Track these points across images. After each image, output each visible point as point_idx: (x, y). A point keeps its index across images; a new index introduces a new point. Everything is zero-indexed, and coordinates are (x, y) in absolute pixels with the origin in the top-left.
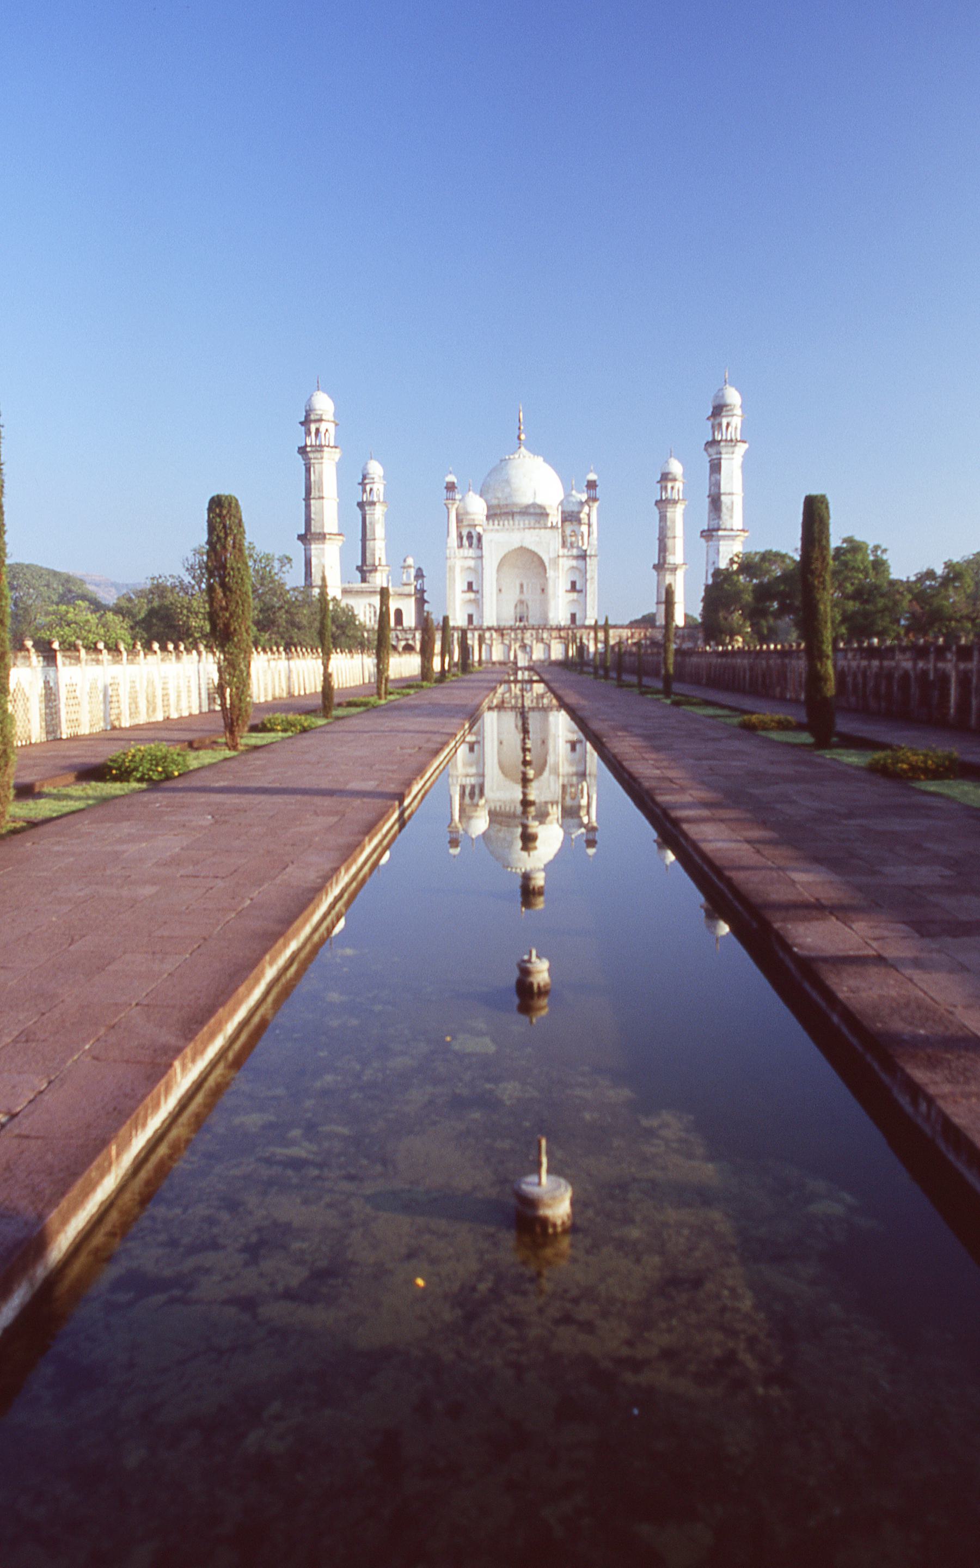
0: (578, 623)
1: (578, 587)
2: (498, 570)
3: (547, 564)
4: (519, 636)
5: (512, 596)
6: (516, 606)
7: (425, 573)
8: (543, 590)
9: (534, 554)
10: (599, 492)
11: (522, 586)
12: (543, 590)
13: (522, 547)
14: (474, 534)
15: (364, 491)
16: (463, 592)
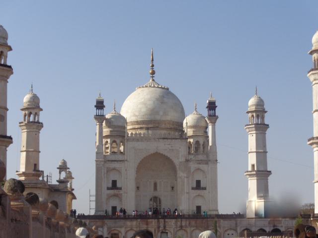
1: (202, 185)
2: (137, 171)
3: (177, 167)
4: (162, 225)
5: (149, 192)
6: (151, 200)
7: (73, 176)
8: (173, 188)
9: (167, 159)
10: (218, 112)
11: (155, 184)
12: (173, 188)
13: (157, 152)
14: (118, 141)
15: (25, 116)
16: (108, 189)
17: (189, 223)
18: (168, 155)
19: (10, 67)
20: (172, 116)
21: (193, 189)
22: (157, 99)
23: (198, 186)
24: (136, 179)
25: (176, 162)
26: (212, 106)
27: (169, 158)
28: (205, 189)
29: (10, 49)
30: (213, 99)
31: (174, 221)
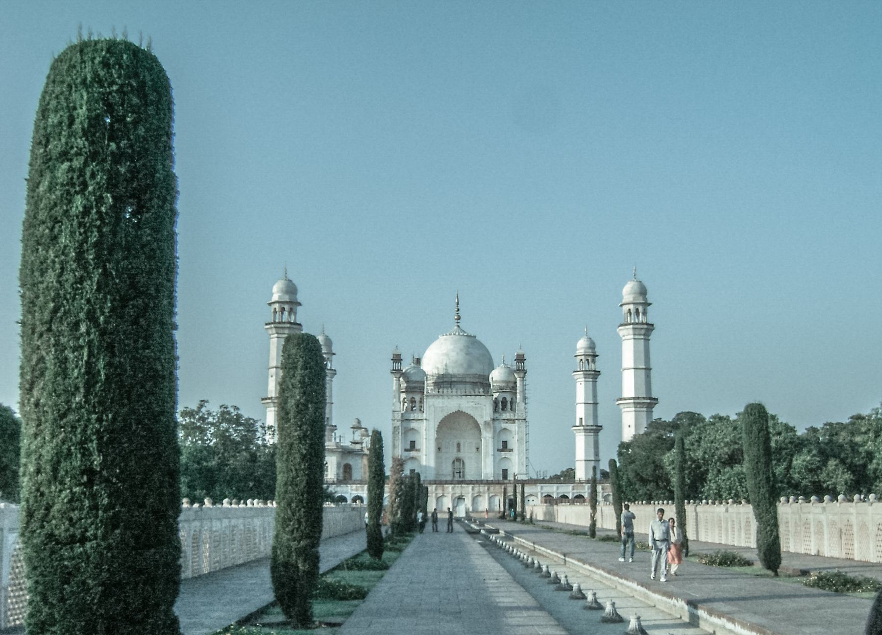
0: (511, 478)
3: (481, 427)
6: (454, 462)
10: (527, 365)
16: (406, 450)
17: (488, 489)
18: (472, 414)
19: (300, 325)
20: (477, 369)
21: (498, 450)
22: (461, 350)
23: (505, 447)
24: (437, 439)
25: (481, 422)
26: (521, 359)
27: (471, 417)
28: (511, 450)
29: (300, 304)
30: (521, 352)
31: (470, 487)
